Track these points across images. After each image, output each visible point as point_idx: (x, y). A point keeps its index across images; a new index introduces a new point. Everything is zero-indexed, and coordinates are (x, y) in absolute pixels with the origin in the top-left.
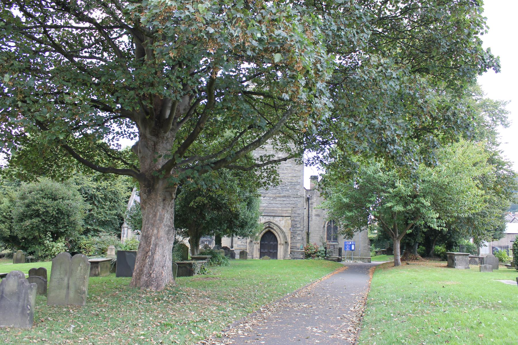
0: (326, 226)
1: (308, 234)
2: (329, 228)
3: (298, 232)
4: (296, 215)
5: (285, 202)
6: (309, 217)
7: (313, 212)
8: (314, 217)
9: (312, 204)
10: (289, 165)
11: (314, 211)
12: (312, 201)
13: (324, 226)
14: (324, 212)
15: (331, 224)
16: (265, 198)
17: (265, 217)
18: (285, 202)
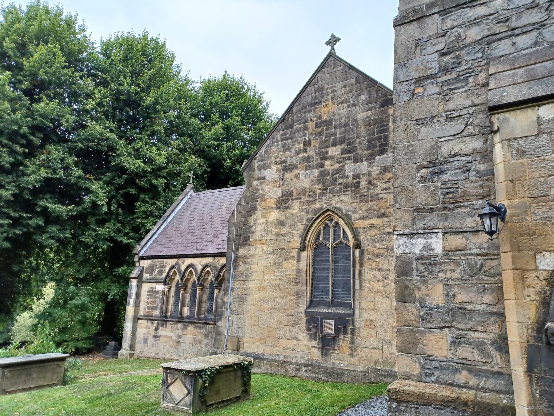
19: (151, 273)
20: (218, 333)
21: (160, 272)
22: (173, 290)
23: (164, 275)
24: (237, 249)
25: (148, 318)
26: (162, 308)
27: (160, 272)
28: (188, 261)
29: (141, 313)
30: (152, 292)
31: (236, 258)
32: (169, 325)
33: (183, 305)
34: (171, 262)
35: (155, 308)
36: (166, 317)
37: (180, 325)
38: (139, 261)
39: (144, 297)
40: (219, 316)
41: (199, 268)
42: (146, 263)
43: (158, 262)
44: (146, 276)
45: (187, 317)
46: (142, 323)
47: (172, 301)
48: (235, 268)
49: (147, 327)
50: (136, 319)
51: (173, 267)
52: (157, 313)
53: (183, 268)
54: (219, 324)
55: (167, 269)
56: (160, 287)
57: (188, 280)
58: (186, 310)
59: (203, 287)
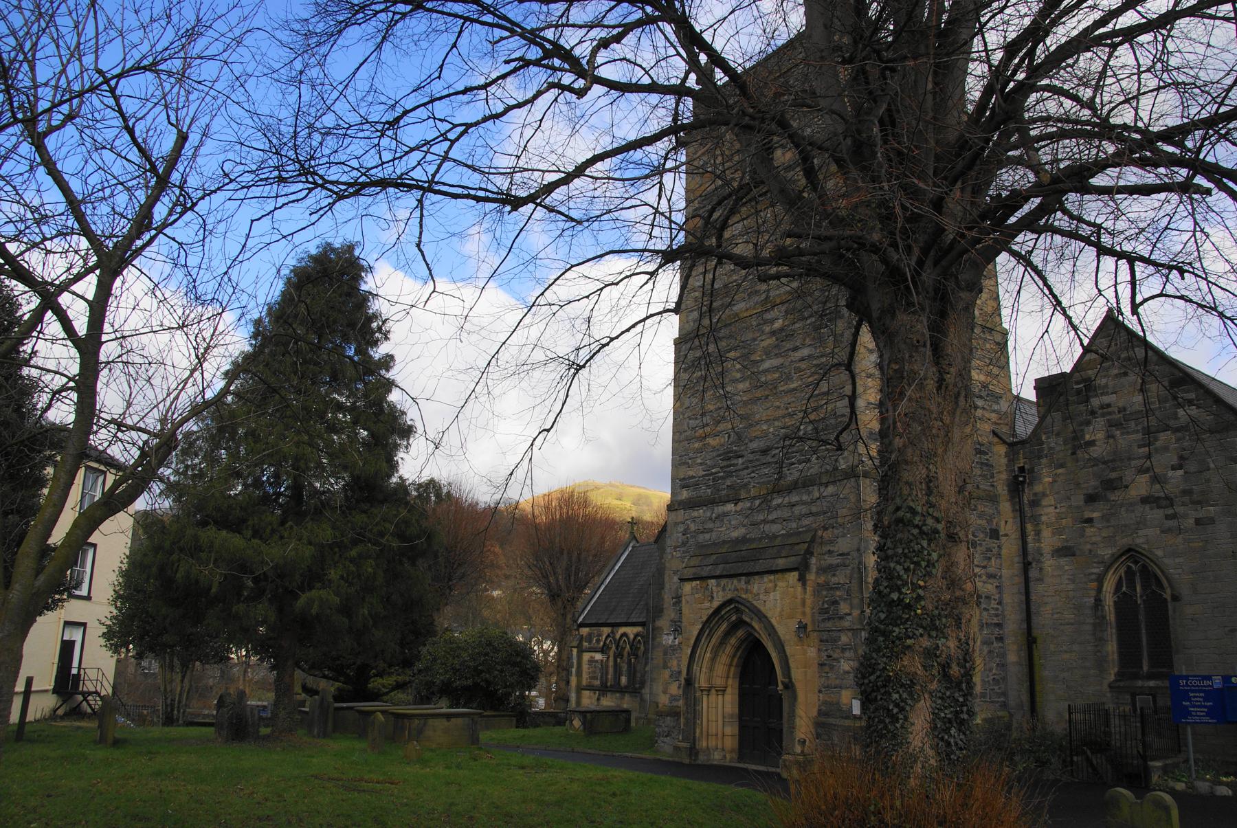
0: (1109, 599)
1: (1030, 641)
2: (1124, 604)
3: (844, 639)
4: (834, 561)
5: (797, 510)
6: (1026, 566)
7: (1048, 540)
8: (1049, 563)
9: (1035, 503)
10: (805, 352)
11: (1046, 533)
12: (1038, 488)
13: (1098, 602)
14: (1090, 531)
15: (1132, 585)
16: (740, 505)
17: (723, 581)
18: (797, 510)
19: (590, 642)
20: (642, 700)
21: (598, 641)
22: (611, 659)
23: (602, 643)
24: (654, 621)
25: (590, 688)
26: (602, 677)
27: (598, 641)
28: (622, 630)
29: (584, 683)
30: (592, 661)
31: (653, 630)
32: (609, 694)
33: (620, 675)
34: (606, 630)
35: (595, 678)
36: (607, 687)
37: (618, 695)
38: (578, 630)
39: (585, 667)
40: (643, 684)
41: (632, 637)
42: (585, 631)
43: (595, 630)
44: (585, 644)
45: (626, 687)
46: (586, 693)
47: (611, 670)
48: (653, 639)
49: (590, 697)
50: (580, 689)
51: (608, 636)
52: (597, 683)
53: (618, 637)
54: (643, 691)
55: (604, 637)
56: (598, 656)
57: (623, 649)
58: (624, 680)
59: (637, 656)
